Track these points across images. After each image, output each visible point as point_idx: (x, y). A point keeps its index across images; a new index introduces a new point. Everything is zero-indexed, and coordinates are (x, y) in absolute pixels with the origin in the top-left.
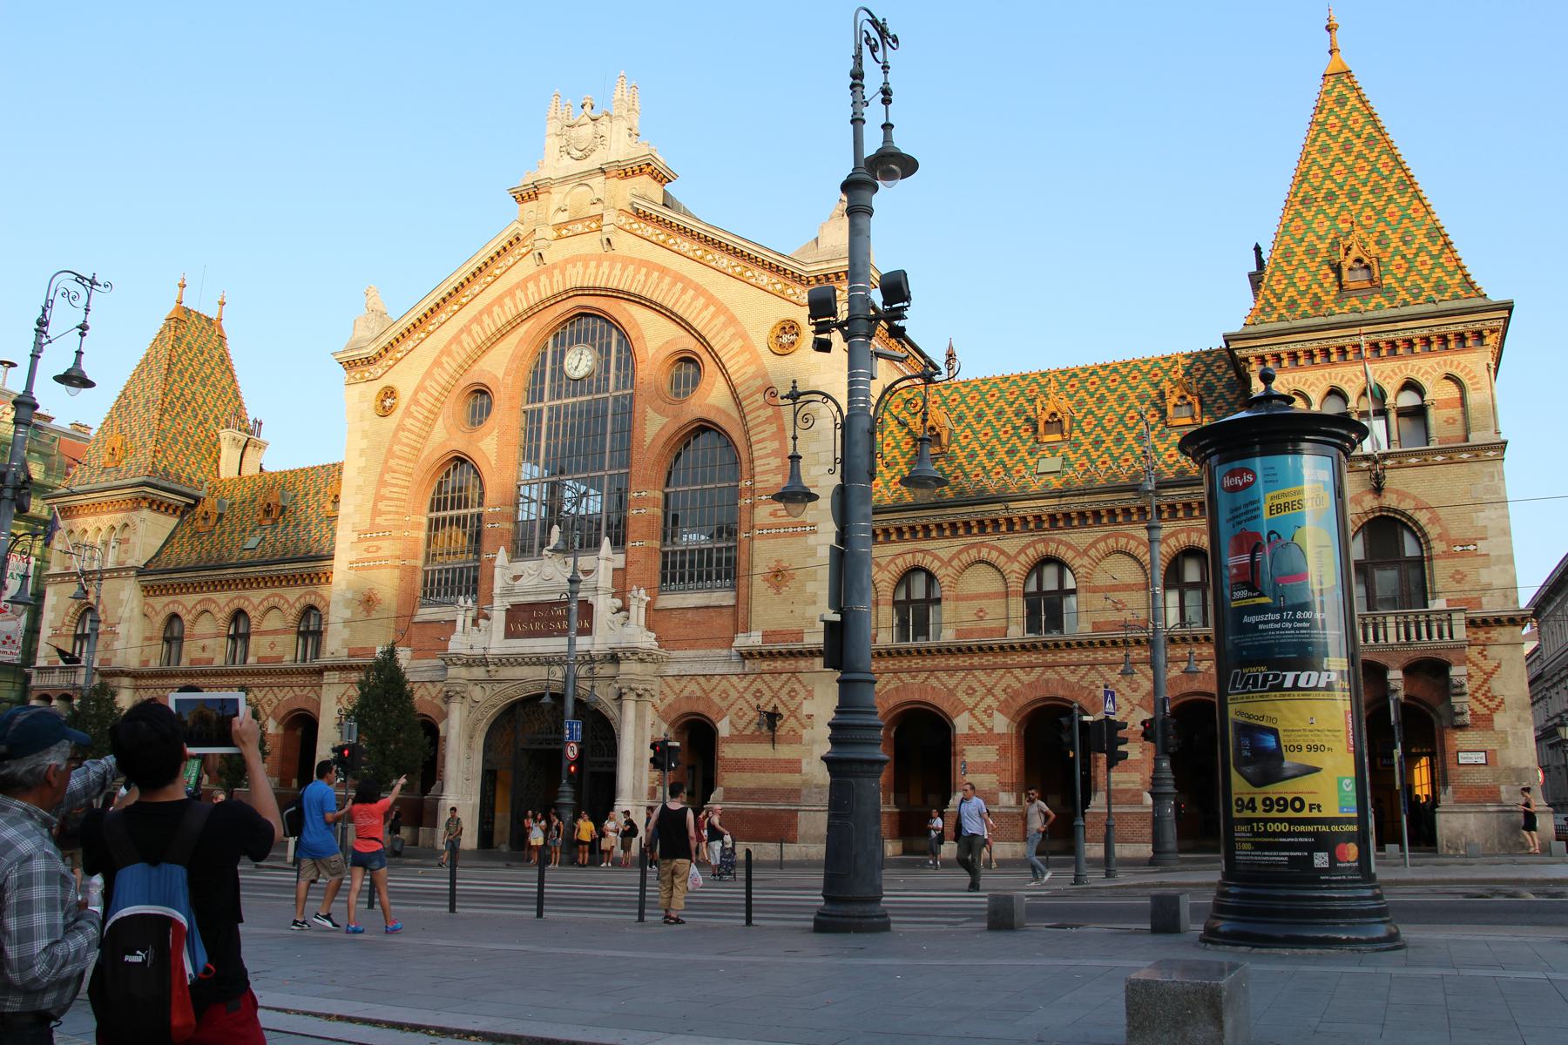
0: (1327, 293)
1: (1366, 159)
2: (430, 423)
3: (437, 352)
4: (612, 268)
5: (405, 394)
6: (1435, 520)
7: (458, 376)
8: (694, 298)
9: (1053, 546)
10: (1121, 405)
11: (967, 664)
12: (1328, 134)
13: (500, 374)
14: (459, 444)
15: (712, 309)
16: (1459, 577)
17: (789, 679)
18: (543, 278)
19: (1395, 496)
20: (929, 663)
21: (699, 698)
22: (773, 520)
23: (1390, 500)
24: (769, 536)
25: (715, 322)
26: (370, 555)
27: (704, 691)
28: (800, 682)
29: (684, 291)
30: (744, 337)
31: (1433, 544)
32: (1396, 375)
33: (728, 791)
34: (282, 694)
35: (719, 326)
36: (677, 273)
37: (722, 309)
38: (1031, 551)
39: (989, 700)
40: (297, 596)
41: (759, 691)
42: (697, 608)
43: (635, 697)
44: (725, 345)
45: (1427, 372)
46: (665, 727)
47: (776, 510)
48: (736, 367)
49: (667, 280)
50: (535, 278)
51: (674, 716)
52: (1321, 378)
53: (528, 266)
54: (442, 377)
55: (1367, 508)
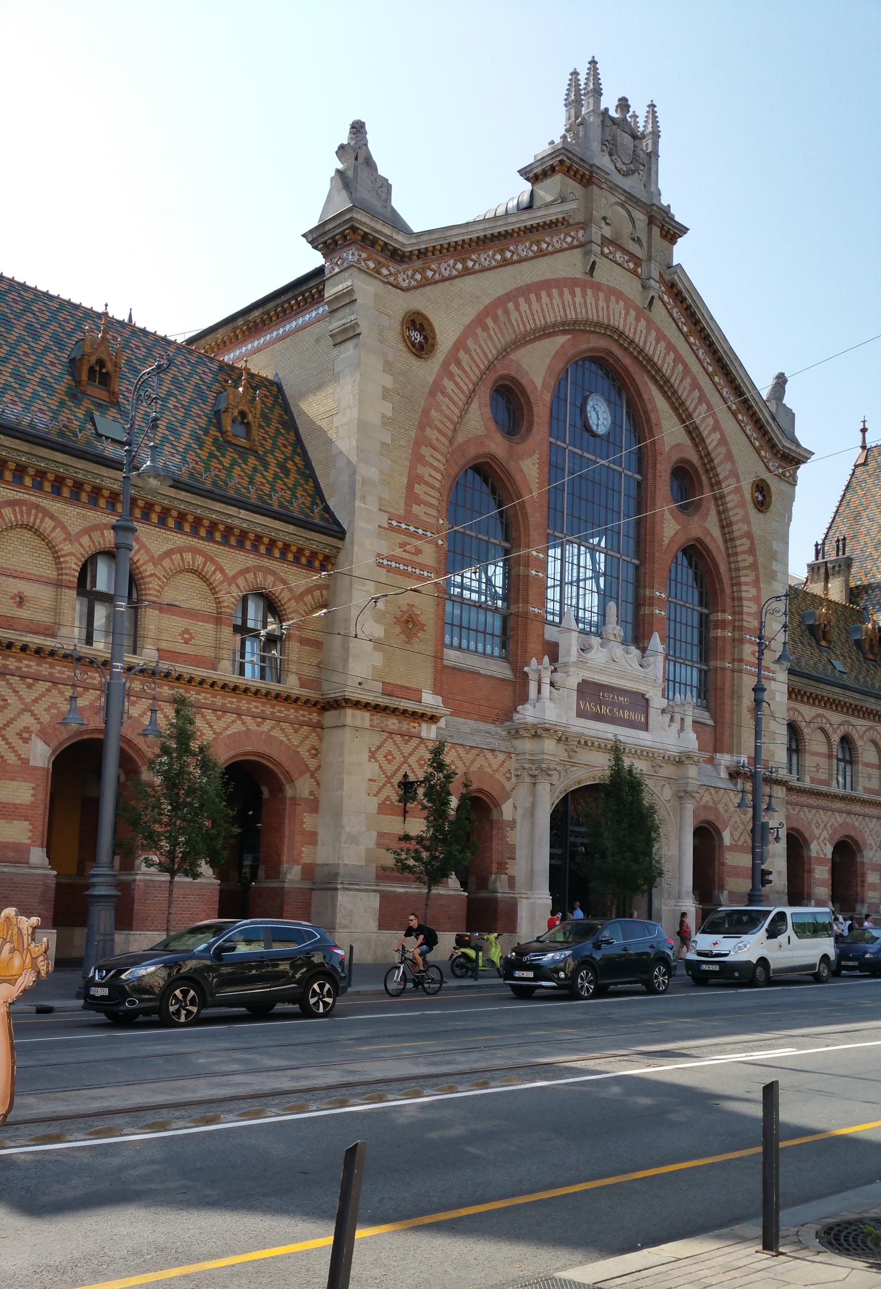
26: (406, 556)
34: (222, 724)
40: (242, 567)
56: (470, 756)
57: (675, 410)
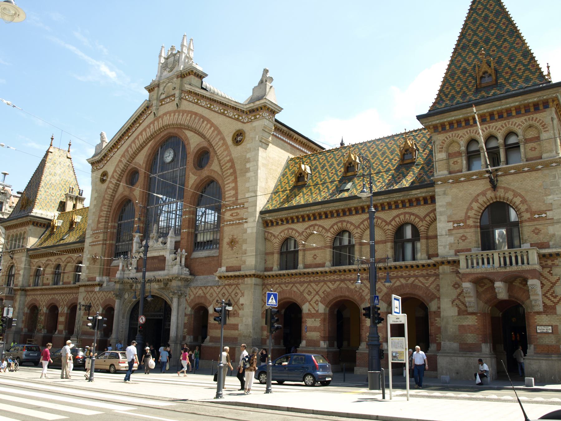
0: (470, 91)
1: (494, 23)
2: (117, 186)
3: (121, 156)
4: (179, 115)
5: (110, 174)
6: (524, 201)
7: (127, 165)
8: (206, 125)
9: (345, 224)
10: (382, 157)
11: (308, 280)
12: (477, 14)
13: (141, 162)
14: (127, 193)
15: (213, 128)
16: (537, 232)
17: (235, 288)
18: (156, 122)
19: (503, 190)
20: (293, 280)
21: (202, 297)
22: (231, 218)
23: (501, 193)
24: (230, 225)
25: (214, 134)
27: (204, 293)
28: (239, 289)
29: (203, 122)
30: (223, 139)
31: (523, 214)
32: (503, 127)
33: (211, 337)
35: (215, 136)
36: (201, 115)
37: (216, 128)
38: (335, 227)
39: (317, 297)
41: (224, 293)
42: (206, 257)
43: (177, 296)
44: (217, 144)
45: (519, 125)
46: (190, 309)
47: (232, 213)
48: (220, 153)
49: (198, 118)
50: (153, 123)
51: (193, 304)
52: (466, 133)
53: (151, 118)
54: (122, 166)
55: (489, 197)
56: (107, 294)
57: (195, 133)
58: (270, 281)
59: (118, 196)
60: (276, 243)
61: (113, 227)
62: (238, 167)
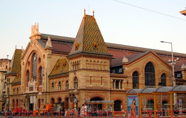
23: (76, 76)
58: (50, 94)
59: (26, 70)
60: (51, 84)
61: (26, 78)
62: (44, 64)
